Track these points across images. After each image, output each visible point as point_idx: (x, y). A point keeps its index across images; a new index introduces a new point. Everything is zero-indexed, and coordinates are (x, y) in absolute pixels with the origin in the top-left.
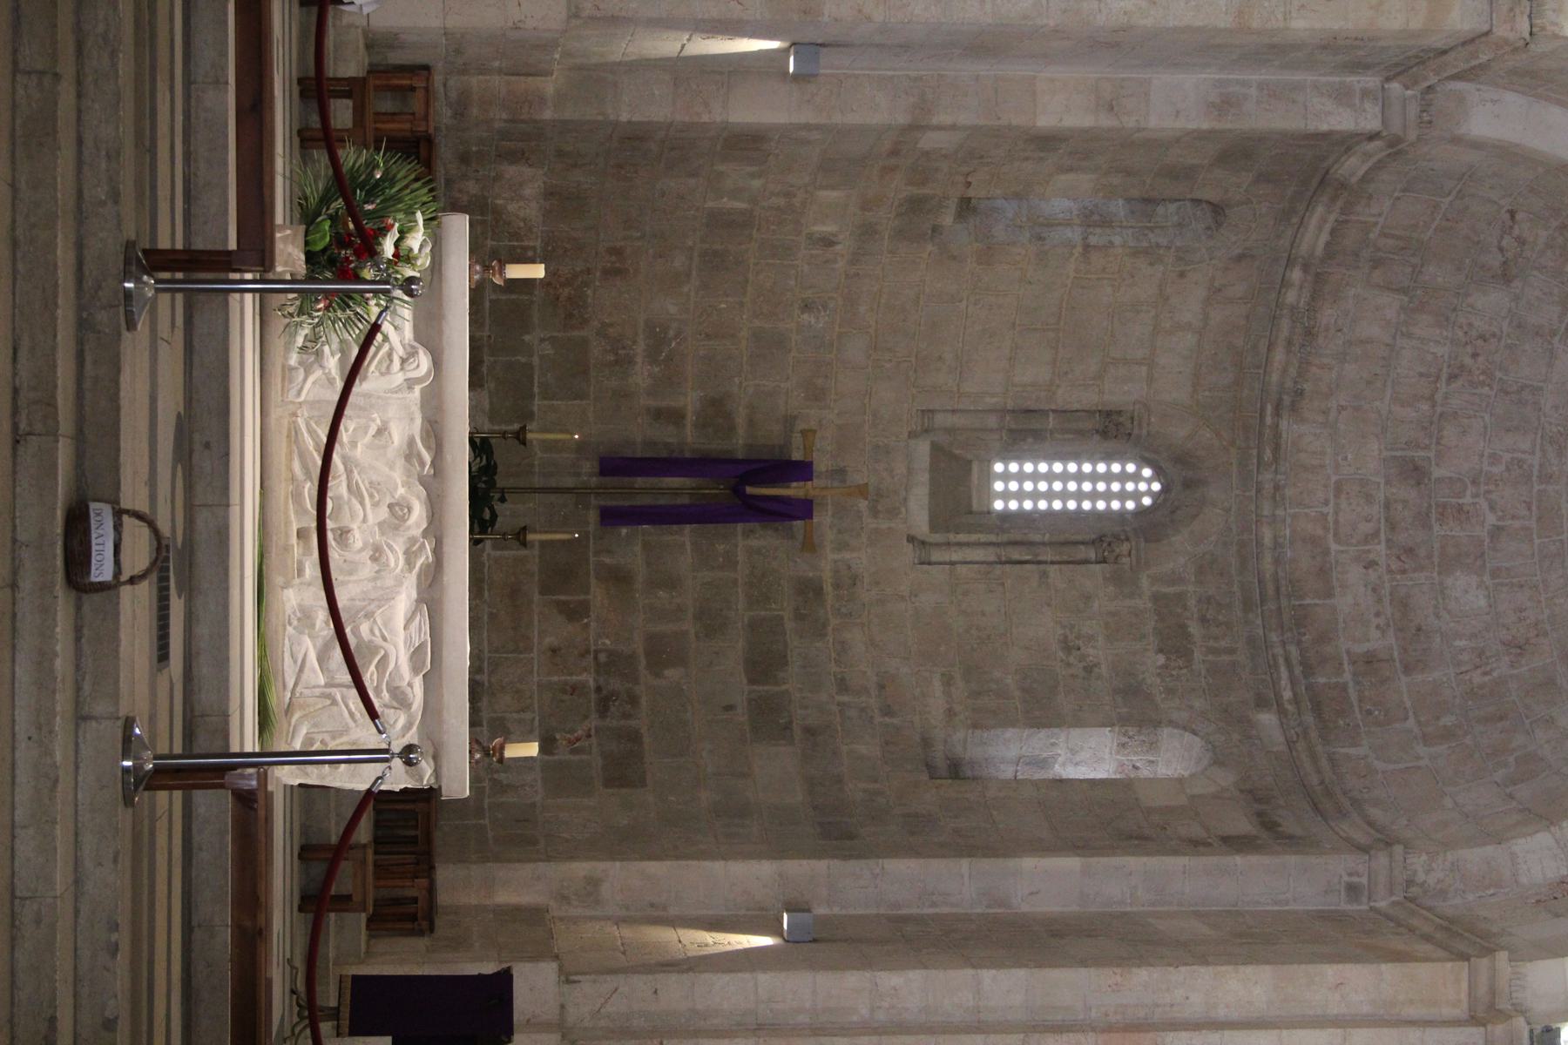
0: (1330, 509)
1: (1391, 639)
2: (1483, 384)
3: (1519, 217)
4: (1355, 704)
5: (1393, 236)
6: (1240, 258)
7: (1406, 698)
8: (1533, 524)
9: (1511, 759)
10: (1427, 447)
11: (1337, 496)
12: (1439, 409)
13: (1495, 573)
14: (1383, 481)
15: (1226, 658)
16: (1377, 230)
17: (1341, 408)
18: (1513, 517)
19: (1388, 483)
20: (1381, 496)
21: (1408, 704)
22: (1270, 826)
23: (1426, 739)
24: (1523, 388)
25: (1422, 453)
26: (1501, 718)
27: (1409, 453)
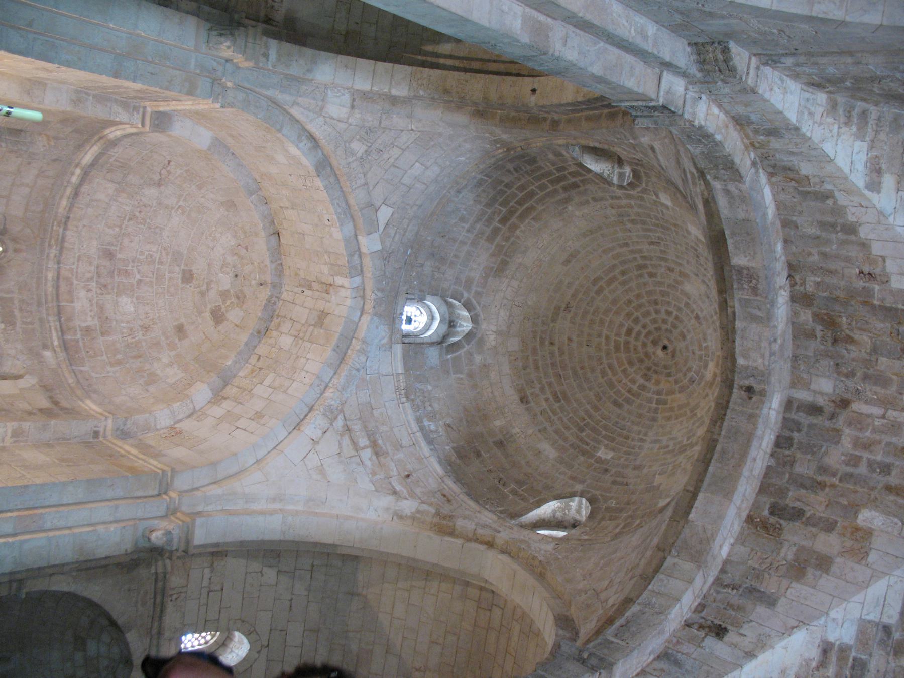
0: (74, 267)
1: (96, 322)
2: (141, 224)
3: (171, 163)
4: (82, 348)
5: (119, 161)
6: (55, 160)
7: (102, 347)
8: (154, 280)
9: (145, 374)
10: (116, 246)
11: (78, 261)
12: (123, 231)
13: (138, 298)
14: (97, 257)
15: (30, 326)
16: (114, 158)
17: (84, 226)
18: (147, 277)
19: (99, 258)
20: (96, 263)
21: (103, 349)
22: (56, 403)
23: (111, 364)
24: (157, 227)
25: (113, 248)
26: (140, 357)
27: (108, 247)
